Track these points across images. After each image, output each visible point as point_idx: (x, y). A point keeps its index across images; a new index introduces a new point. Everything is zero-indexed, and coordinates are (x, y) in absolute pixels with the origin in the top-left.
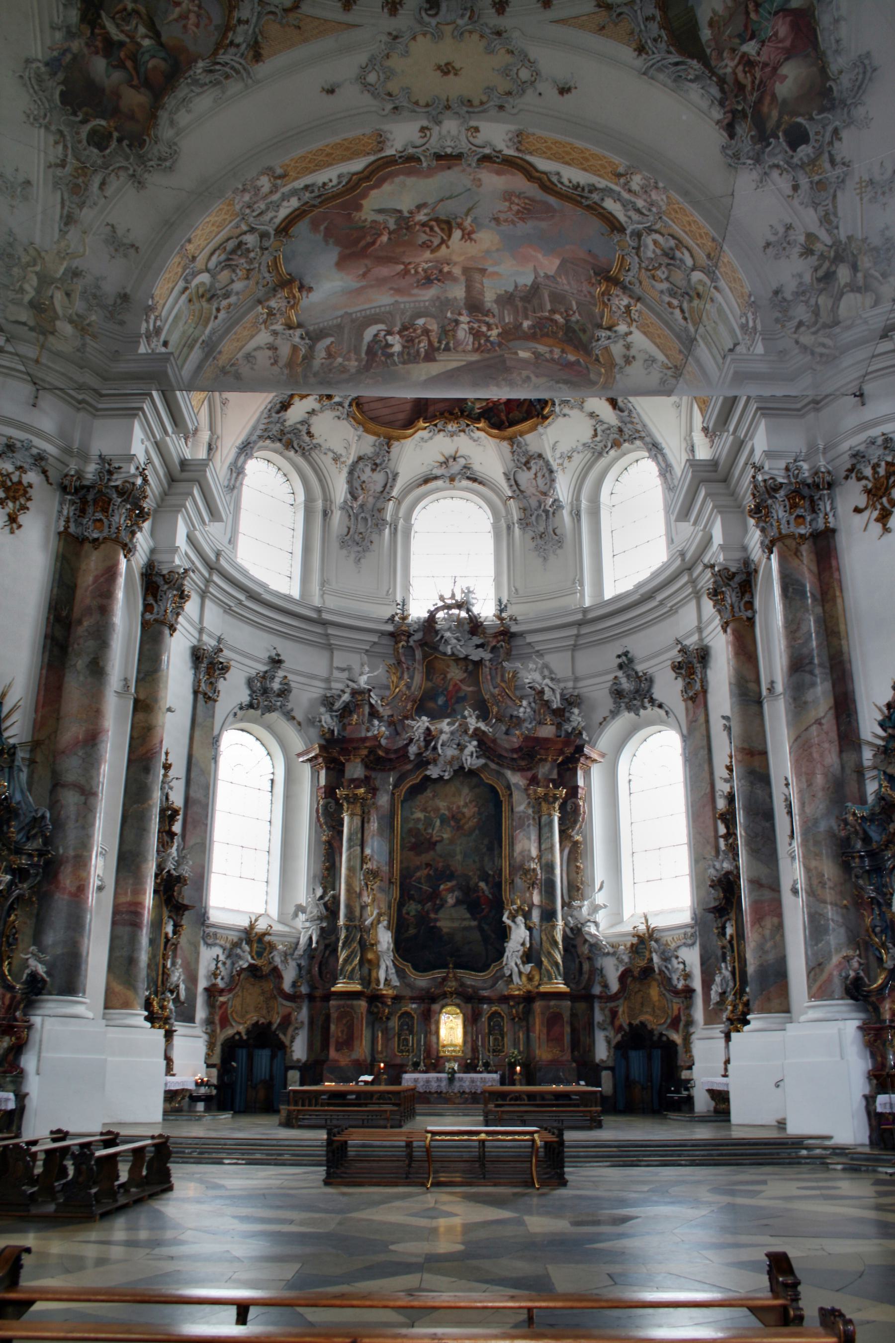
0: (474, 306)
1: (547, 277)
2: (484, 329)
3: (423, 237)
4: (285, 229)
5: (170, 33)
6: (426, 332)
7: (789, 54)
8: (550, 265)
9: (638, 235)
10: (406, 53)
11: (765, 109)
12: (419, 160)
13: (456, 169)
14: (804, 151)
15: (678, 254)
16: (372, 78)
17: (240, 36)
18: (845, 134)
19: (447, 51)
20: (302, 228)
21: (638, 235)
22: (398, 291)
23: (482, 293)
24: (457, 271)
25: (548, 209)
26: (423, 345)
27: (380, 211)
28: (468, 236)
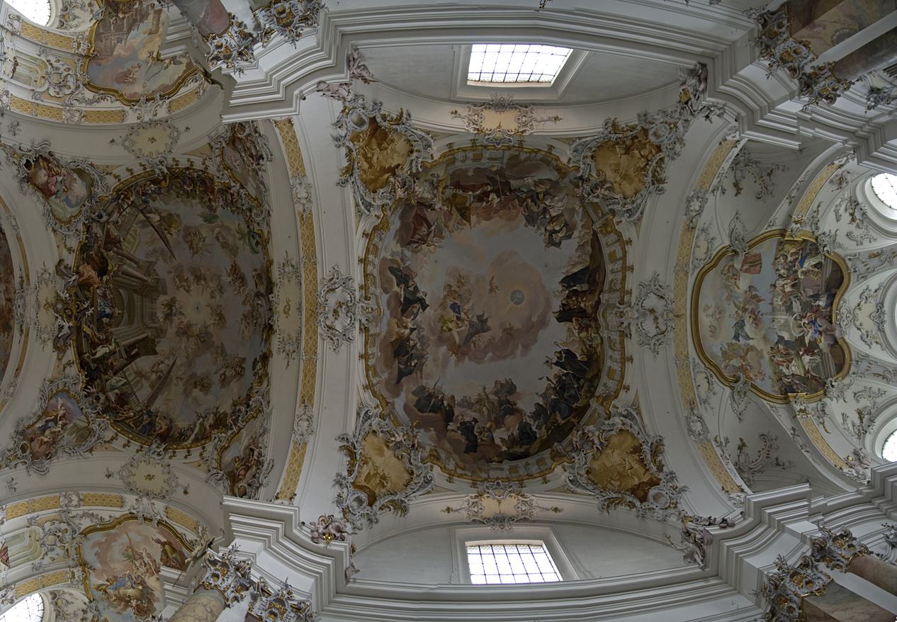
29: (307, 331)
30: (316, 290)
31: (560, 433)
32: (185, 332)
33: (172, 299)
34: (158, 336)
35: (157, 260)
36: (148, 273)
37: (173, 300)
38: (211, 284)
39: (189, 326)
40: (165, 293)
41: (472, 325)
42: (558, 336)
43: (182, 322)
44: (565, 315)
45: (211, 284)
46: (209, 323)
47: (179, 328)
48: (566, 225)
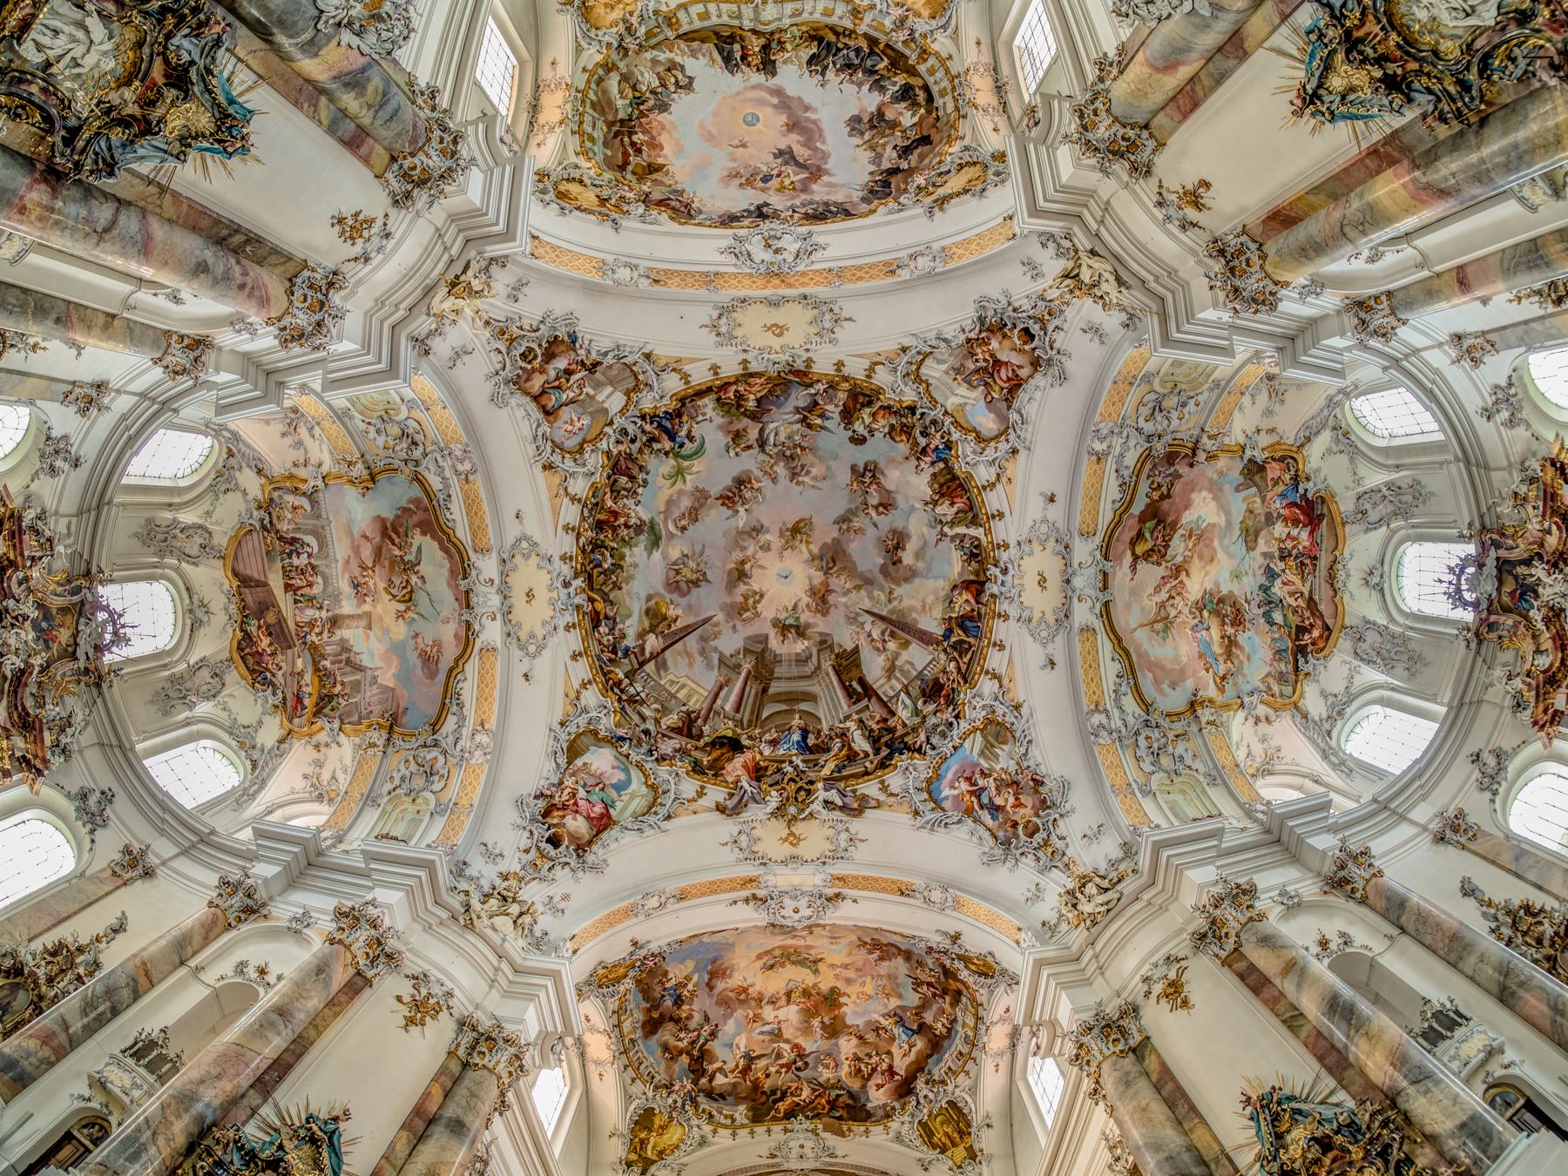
0: (335, 622)
1: (375, 678)
2: (317, 630)
3: (397, 581)
4: (418, 479)
5: (565, 413)
6: (310, 585)
7: (588, 818)
8: (387, 678)
9: (436, 744)
10: (539, 567)
11: (555, 813)
12: (465, 578)
13: (456, 605)
14: (549, 847)
15: (436, 778)
16: (524, 544)
17: (557, 458)
18: (567, 869)
19: (542, 595)
20: (416, 491)
21: (436, 744)
22: (347, 562)
23: (348, 627)
24: (366, 607)
25: (432, 675)
26: (297, 582)
27: (419, 549)
28: (400, 615)
29: (803, 284)
30: (751, 275)
31: (898, 61)
32: (821, 599)
33: (775, 626)
34: (831, 647)
35: (716, 649)
36: (737, 668)
37: (776, 623)
38: (750, 552)
39: (813, 592)
40: (767, 637)
41: (786, 163)
42: (792, 75)
43: (808, 605)
44: (768, 66)
45: (750, 552)
46: (806, 555)
47: (817, 611)
48: (669, 70)
